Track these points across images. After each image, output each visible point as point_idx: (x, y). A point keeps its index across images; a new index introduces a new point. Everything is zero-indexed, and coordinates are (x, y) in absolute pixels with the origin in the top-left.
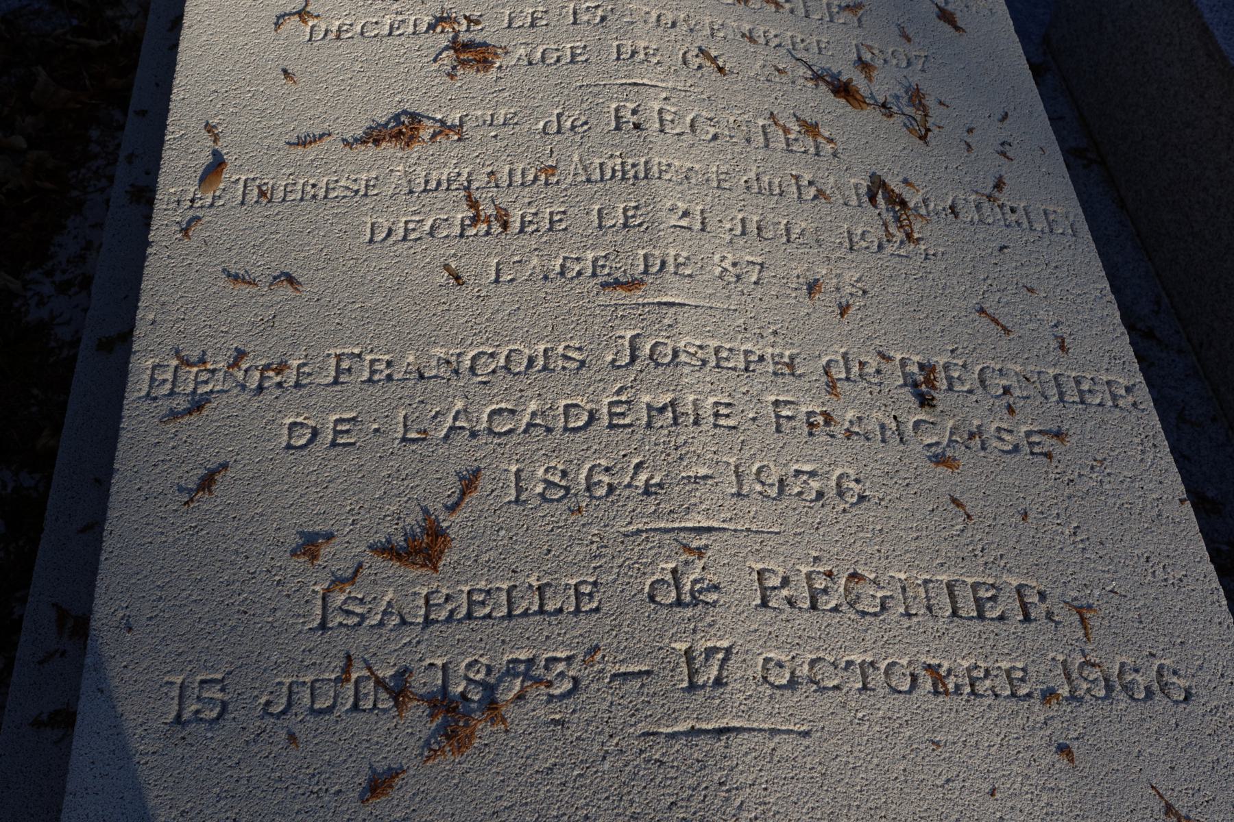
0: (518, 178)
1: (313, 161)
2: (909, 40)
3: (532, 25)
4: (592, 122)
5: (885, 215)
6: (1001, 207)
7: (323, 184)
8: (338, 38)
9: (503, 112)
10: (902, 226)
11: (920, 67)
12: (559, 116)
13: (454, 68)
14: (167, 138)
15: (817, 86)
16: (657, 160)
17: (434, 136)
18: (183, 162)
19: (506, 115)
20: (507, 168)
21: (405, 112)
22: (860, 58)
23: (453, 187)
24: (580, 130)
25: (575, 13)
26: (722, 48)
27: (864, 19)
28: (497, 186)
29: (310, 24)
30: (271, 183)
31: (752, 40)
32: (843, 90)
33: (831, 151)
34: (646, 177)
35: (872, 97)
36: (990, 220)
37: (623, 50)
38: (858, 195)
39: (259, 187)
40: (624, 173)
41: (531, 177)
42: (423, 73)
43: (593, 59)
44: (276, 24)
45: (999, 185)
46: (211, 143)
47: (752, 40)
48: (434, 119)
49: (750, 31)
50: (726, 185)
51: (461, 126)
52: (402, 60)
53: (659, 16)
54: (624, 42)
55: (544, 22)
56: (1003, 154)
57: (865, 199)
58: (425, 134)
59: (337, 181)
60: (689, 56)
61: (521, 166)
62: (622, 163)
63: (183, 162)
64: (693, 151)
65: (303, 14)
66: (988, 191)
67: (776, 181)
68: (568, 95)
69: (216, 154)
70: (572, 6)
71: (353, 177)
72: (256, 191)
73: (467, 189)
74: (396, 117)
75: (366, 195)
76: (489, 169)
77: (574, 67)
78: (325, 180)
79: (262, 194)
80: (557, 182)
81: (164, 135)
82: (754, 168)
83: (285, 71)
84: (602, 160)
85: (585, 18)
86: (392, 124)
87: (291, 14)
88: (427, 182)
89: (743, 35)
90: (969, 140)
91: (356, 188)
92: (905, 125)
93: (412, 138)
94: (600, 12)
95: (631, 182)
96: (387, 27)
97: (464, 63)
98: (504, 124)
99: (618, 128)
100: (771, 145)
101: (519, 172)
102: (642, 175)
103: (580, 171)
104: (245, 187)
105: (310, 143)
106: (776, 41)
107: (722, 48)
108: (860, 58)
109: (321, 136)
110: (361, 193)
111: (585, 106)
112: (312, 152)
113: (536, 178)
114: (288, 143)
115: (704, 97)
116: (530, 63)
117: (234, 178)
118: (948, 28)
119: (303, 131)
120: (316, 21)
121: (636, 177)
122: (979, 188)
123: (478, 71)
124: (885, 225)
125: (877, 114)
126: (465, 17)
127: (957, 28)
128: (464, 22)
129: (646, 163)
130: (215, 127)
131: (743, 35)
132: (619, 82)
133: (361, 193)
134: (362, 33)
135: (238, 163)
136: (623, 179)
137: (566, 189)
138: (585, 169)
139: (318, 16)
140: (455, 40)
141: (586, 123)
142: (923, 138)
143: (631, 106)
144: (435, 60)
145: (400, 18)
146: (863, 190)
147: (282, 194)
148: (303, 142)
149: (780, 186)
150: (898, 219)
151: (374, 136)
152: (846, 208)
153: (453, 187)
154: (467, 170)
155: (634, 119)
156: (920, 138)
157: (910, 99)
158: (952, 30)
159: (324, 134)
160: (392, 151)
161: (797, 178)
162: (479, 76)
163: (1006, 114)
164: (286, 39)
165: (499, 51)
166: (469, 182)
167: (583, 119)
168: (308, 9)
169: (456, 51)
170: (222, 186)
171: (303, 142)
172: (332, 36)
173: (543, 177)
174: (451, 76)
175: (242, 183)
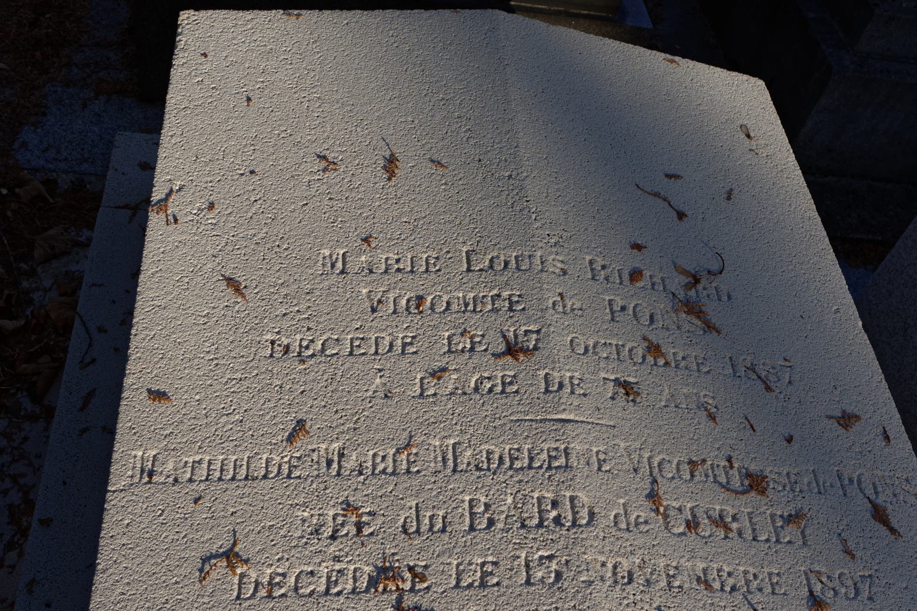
2: (853, 557)
3: (483, 585)
8: (270, 596)
11: (867, 593)
22: (811, 592)
25: (527, 566)
27: (807, 532)
29: (239, 571)
31: (708, 587)
44: (201, 570)
47: (708, 587)
49: (705, 571)
53: (615, 567)
55: (495, 580)
70: (523, 555)
85: (540, 574)
87: (216, 556)
89: (699, 580)
94: (554, 566)
96: (324, 580)
106: (731, 581)
108: (811, 592)
118: (883, 531)
120: (245, 568)
126: (411, 569)
127: (893, 530)
128: (408, 575)
131: (699, 580)
134: (296, 589)
139: (246, 561)
145: (338, 567)
158: (888, 532)
164: (212, 595)
168: (236, 549)
172: (263, 593)
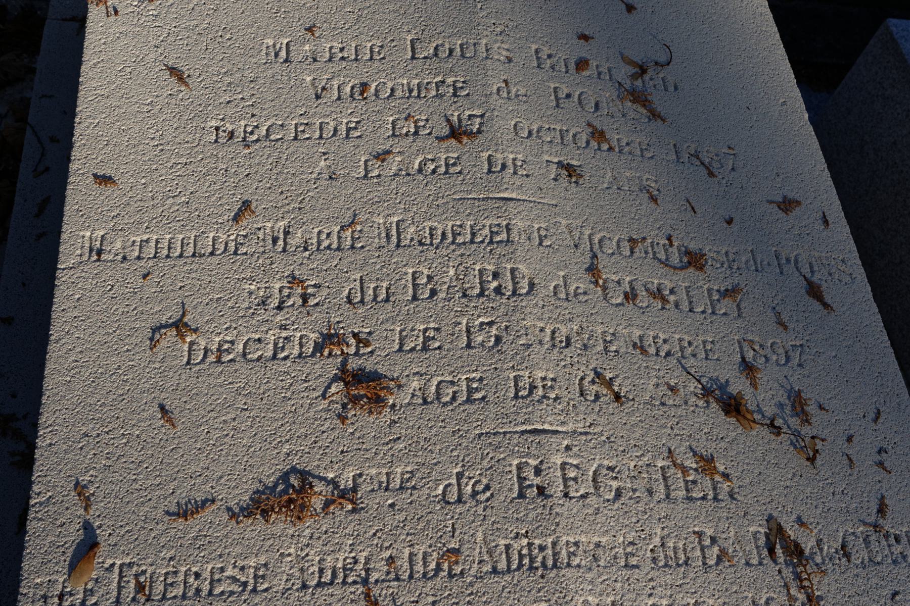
0: (419, 568)
1: (196, 538)
2: (786, 328)
3: (425, 348)
4: (495, 486)
5: (784, 571)
6: (887, 536)
7: (206, 575)
8: (219, 361)
9: (399, 470)
10: (803, 587)
11: (797, 361)
12: (460, 476)
13: (344, 406)
14: (32, 502)
15: (707, 402)
16: (564, 539)
17: (327, 504)
18: (50, 539)
19: (402, 474)
20: (407, 551)
21: (294, 470)
22: (743, 359)
23: (350, 580)
24: (483, 497)
25: (468, 331)
26: (615, 368)
27: (743, 305)
28: (397, 579)
29: (188, 339)
30: (149, 571)
31: (644, 351)
32: (733, 407)
33: (727, 489)
34: (555, 566)
35: (760, 411)
36: (879, 559)
37: (521, 384)
38: (757, 547)
39: (137, 576)
40: (532, 560)
41: (433, 566)
42: (311, 414)
43: (491, 397)
44: (151, 339)
45: (882, 510)
46: (82, 512)
47: (644, 351)
48: (325, 479)
49: (641, 338)
50: (633, 561)
51: (355, 490)
52: (289, 394)
53: (553, 332)
54: (521, 373)
55: (437, 344)
56: (881, 464)
57: (765, 552)
58: (317, 503)
59: (222, 570)
60: (586, 382)
61: (423, 548)
62: (530, 545)
63: (50, 539)
64: (600, 518)
65: (180, 326)
66: (871, 520)
67: (680, 545)
68: (467, 448)
69: (87, 527)
70: (464, 322)
71: (240, 563)
72: (132, 584)
73: (365, 582)
74: (285, 477)
75: (254, 590)
76: (387, 554)
77: (471, 408)
78: (210, 567)
79: (140, 588)
80: (462, 572)
81: (29, 498)
82: (659, 531)
83: (162, 407)
84: (508, 542)
85: (480, 339)
86: (281, 487)
87: (166, 326)
88: (321, 571)
89: (635, 346)
90: (850, 452)
91: (243, 579)
92: (792, 443)
93: (303, 507)
94: (494, 331)
95: (540, 572)
96: (271, 346)
97: (355, 400)
98: (401, 488)
99: (521, 495)
100: (673, 494)
101: (420, 556)
102: (550, 563)
103: (486, 557)
104: (121, 576)
105: (192, 513)
106: (666, 347)
107: (615, 368)
108: (743, 359)
109: (204, 502)
110: (250, 588)
111: (485, 463)
112: (195, 525)
113: (439, 568)
114: (167, 513)
115: (604, 438)
116: (425, 402)
117: (109, 562)
118: (817, 305)
119: (182, 495)
120: (194, 336)
121: (544, 565)
122: (864, 516)
123: (371, 412)
124: (786, 586)
125: (765, 432)
126: (355, 335)
127: (826, 305)
128: (352, 341)
129: (554, 544)
130: (85, 487)
131: (635, 346)
132: (519, 429)
133: (250, 588)
134: (244, 355)
135: (112, 540)
136: (531, 568)
137: (471, 584)
138: (490, 553)
139: (195, 330)
140: (343, 367)
141: (487, 488)
142: (812, 460)
143: (533, 462)
144: (324, 396)
145: (284, 334)
146: (762, 540)
147: (162, 588)
148: (184, 513)
149: (685, 550)
150: (798, 577)
151: (260, 506)
152: (748, 569)
153: (350, 580)
154: (365, 554)
155: (537, 481)
156: (808, 459)
157: (793, 406)
158: (821, 307)
159: (207, 500)
160: (281, 526)
161: (700, 534)
162: (372, 419)
163: (879, 410)
164: (162, 361)
165: (392, 384)
166: (367, 571)
167: (485, 481)
168: (185, 320)
169: (346, 384)
170: (94, 575)
171: (184, 513)
172: (212, 358)
173: (446, 566)
174: (343, 418)
175: (116, 570)
